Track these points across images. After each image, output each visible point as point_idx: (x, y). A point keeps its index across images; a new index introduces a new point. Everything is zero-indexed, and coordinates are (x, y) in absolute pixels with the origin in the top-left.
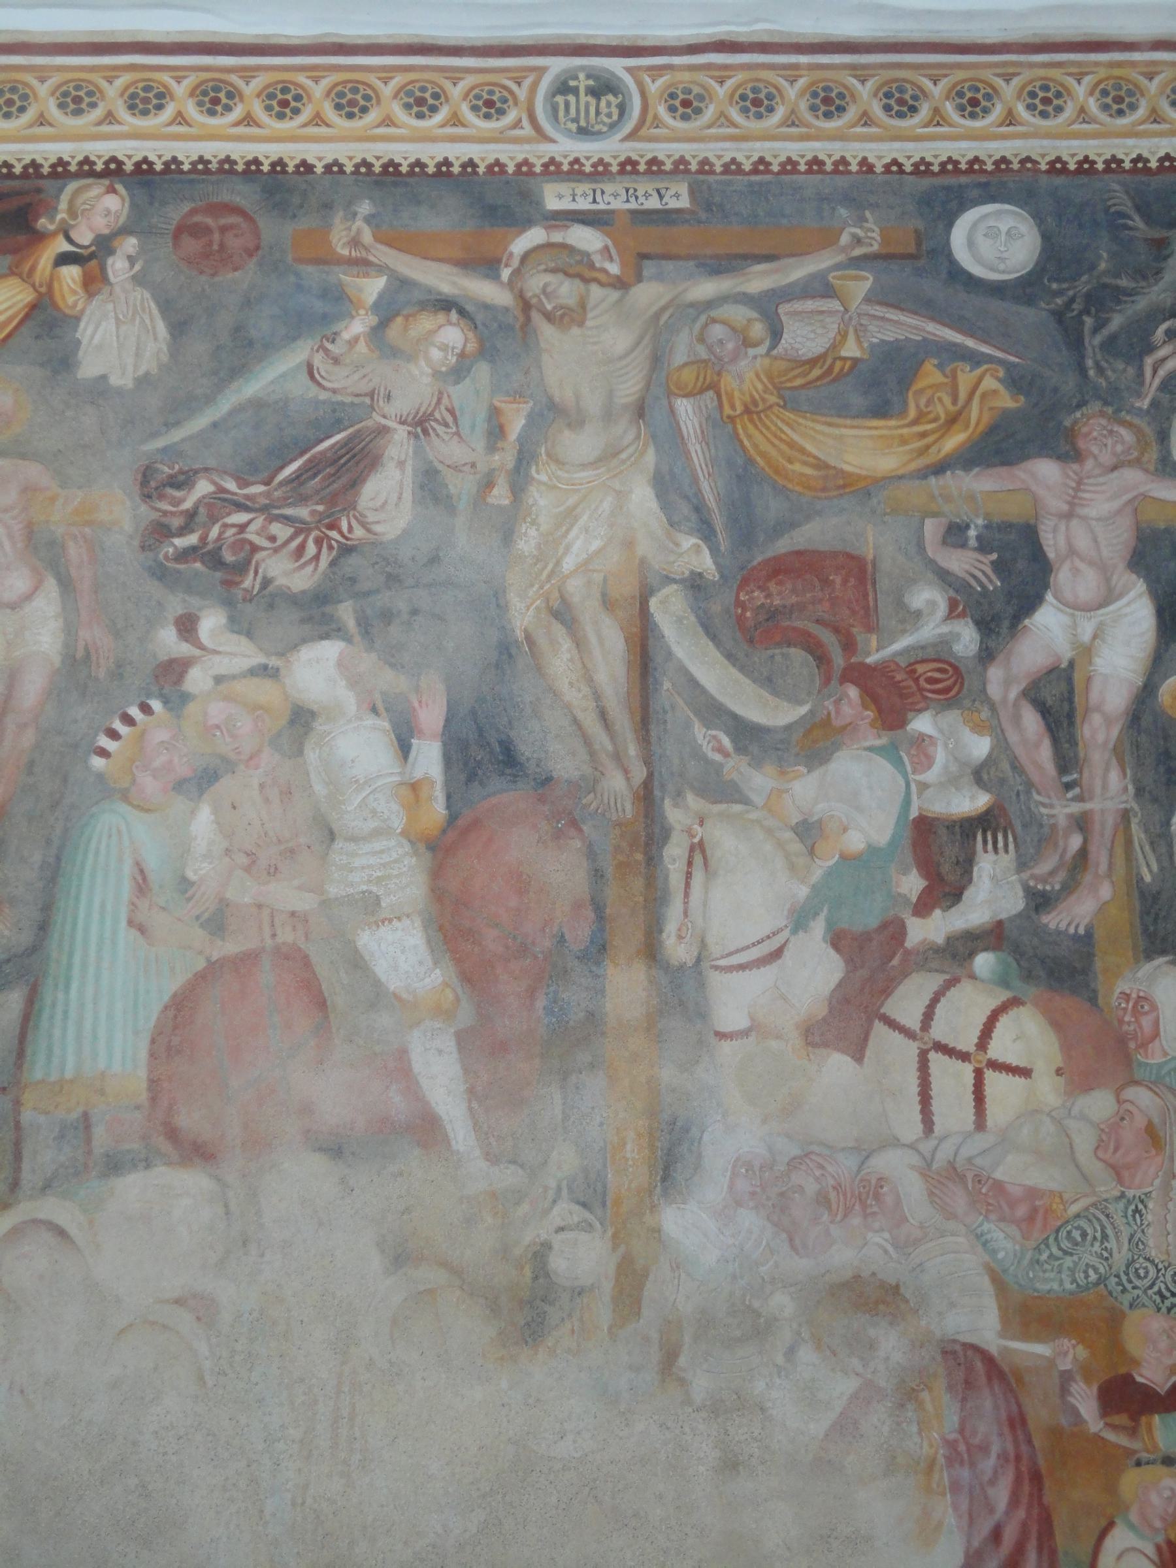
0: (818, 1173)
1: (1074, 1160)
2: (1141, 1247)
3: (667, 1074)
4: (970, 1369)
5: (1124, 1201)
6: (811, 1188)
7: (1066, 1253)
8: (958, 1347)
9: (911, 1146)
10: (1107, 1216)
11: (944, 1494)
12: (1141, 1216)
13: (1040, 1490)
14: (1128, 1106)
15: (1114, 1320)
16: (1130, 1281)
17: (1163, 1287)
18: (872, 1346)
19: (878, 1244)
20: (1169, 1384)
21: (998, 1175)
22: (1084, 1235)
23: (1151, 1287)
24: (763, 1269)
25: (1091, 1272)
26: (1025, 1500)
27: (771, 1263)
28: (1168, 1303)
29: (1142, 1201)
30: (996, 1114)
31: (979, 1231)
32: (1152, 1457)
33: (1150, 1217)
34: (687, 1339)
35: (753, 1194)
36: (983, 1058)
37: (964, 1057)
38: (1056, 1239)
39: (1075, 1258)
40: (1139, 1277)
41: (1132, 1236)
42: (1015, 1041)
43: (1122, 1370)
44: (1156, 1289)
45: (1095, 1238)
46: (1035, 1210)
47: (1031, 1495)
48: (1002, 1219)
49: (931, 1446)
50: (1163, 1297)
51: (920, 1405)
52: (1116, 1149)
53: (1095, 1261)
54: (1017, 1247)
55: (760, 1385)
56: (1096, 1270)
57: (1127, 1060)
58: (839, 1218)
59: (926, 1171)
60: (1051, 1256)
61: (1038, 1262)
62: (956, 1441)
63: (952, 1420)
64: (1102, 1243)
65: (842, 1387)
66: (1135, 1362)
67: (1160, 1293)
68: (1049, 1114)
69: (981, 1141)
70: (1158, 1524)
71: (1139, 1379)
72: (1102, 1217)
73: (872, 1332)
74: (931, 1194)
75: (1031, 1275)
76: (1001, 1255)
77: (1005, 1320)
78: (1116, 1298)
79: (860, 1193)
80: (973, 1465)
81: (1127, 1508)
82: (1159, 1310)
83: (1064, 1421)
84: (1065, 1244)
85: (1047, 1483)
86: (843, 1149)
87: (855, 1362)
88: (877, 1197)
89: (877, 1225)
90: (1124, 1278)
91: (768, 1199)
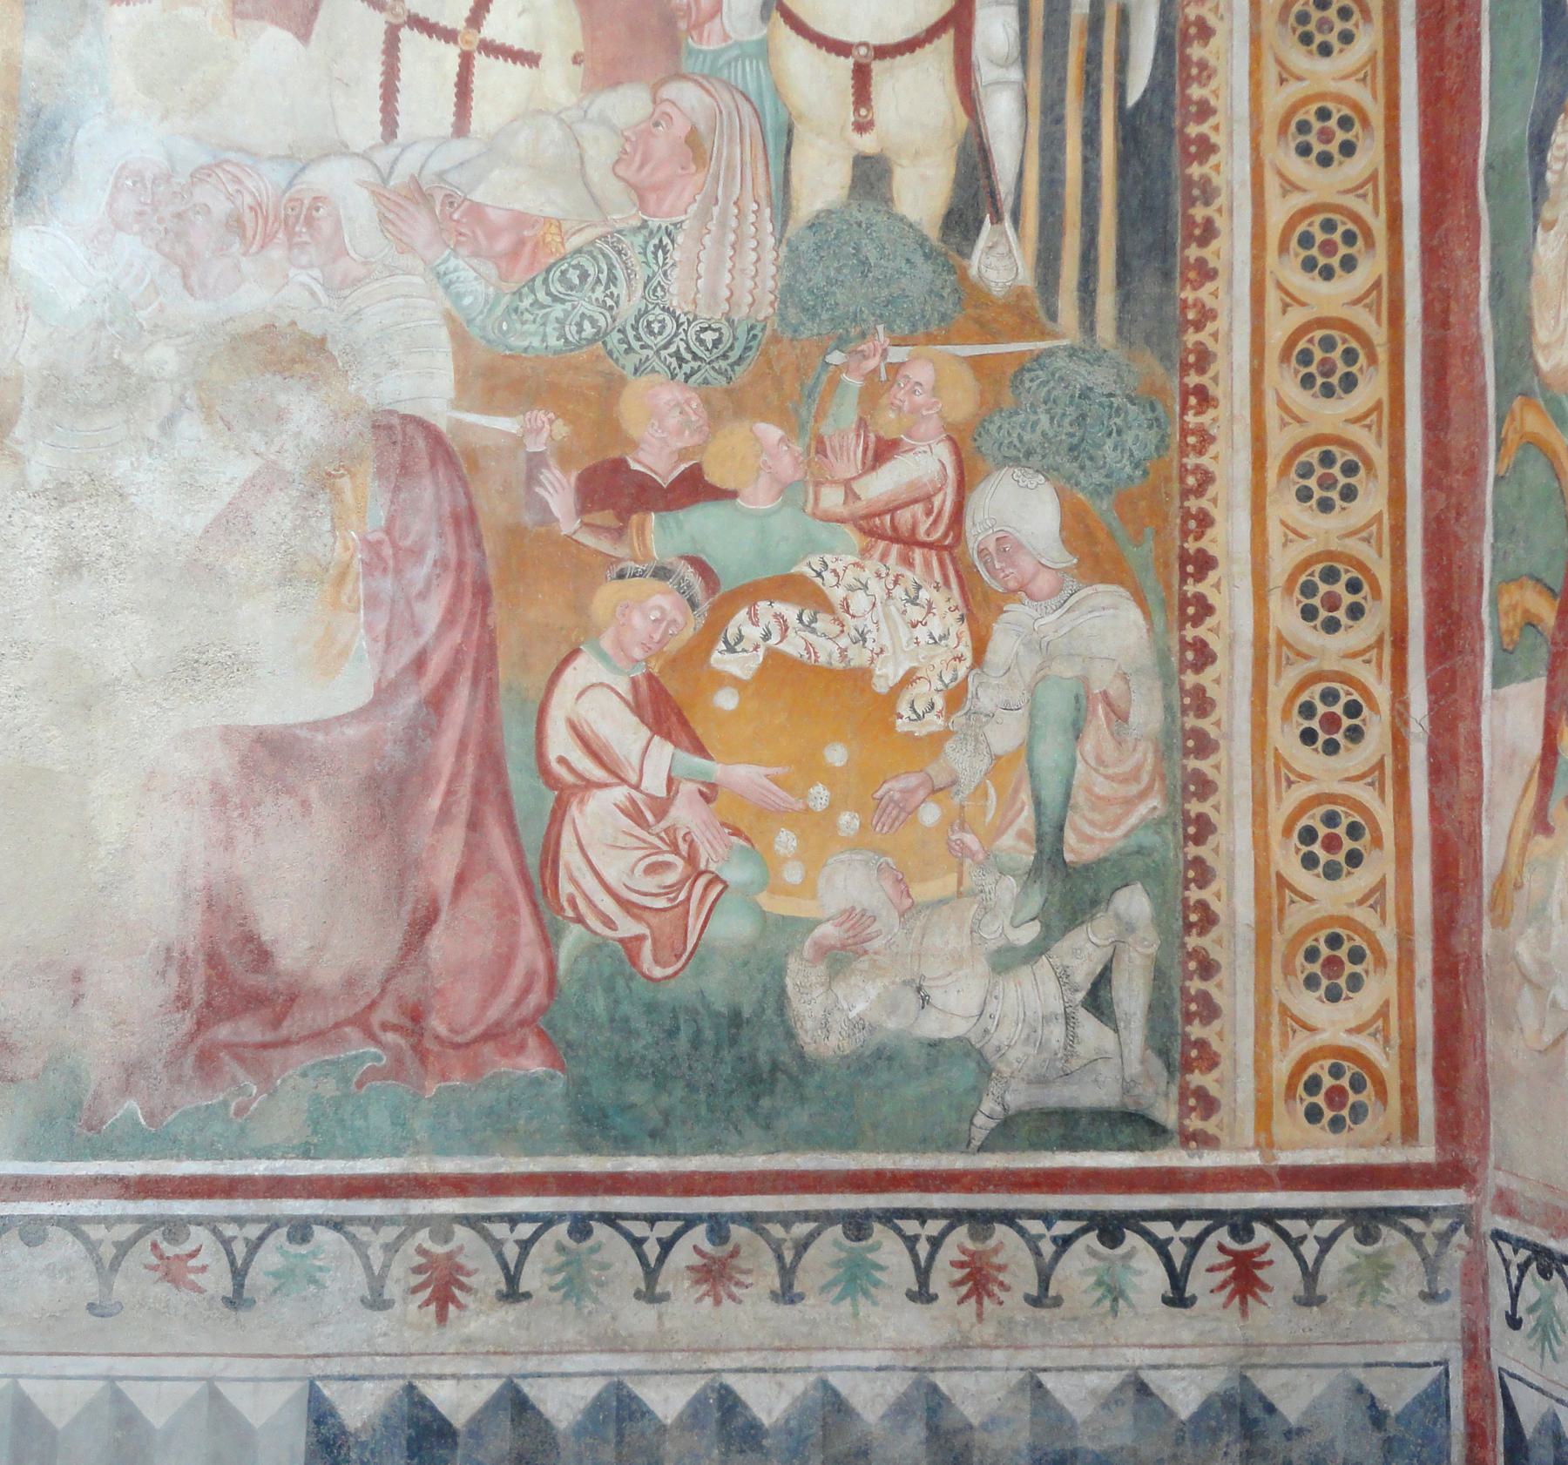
0: (231, 188)
1: (583, 174)
2: (659, 293)
3: (33, 49)
4: (408, 450)
5: (645, 232)
6: (221, 207)
7: (556, 299)
8: (395, 421)
9: (365, 156)
10: (619, 253)
11: (357, 610)
12: (665, 253)
13: (485, 607)
14: (668, 108)
15: (612, 387)
16: (639, 338)
17: (682, 346)
18: (280, 417)
19: (303, 285)
20: (676, 473)
21: (478, 196)
22: (584, 276)
23: (666, 347)
24: (142, 315)
25: (587, 325)
26: (463, 619)
27: (156, 305)
28: (686, 368)
29: (669, 234)
30: (484, 114)
31: (442, 269)
32: (640, 568)
33: (677, 256)
34: (28, 402)
35: (141, 214)
36: (474, 38)
37: (449, 36)
38: (545, 281)
39: (568, 306)
40: (651, 333)
41: (649, 279)
42: (520, 15)
43: (614, 454)
44: (673, 349)
45: (598, 281)
46: (521, 242)
47: (472, 615)
48: (475, 254)
49: (346, 548)
50: (681, 360)
51: (337, 494)
52: (642, 167)
53: (586, 307)
54: (491, 290)
55: (123, 466)
56: (593, 322)
57: (674, 47)
58: (254, 248)
59: (380, 193)
60: (536, 303)
61: (516, 310)
62: (380, 543)
63: (378, 515)
64: (607, 287)
65: (234, 471)
66: (634, 445)
67: (677, 355)
68: (557, 116)
69: (461, 149)
70: (638, 653)
71: (635, 466)
72: (613, 255)
73: (282, 399)
74: (383, 219)
75: (505, 327)
76: (467, 301)
77: (462, 383)
78: (617, 360)
79: (287, 216)
80: (398, 572)
81: (599, 633)
82: (673, 376)
83: (528, 519)
84: (557, 288)
85: (497, 596)
86: (272, 158)
87: (255, 439)
88: (310, 221)
89: (304, 260)
90: (631, 334)
91: (161, 220)
